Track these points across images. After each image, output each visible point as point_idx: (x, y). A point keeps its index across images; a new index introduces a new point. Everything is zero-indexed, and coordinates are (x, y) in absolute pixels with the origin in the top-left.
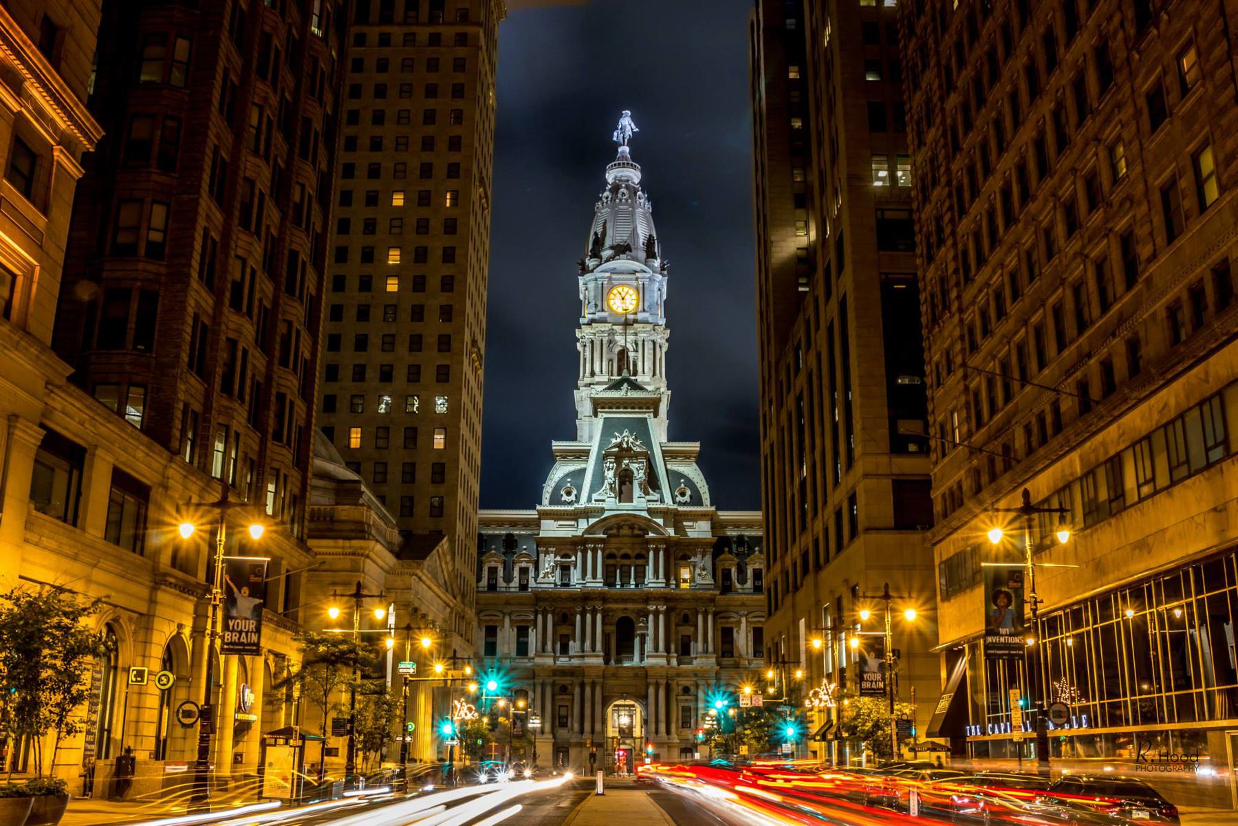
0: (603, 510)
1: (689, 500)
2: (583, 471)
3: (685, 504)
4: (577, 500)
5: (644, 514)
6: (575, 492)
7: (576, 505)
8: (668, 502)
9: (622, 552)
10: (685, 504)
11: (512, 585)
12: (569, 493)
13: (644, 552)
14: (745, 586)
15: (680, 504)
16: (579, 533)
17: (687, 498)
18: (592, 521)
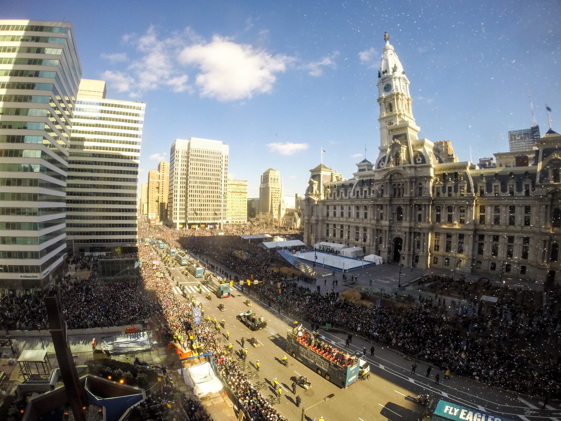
0: (388, 169)
3: (420, 163)
10: (420, 163)
15: (418, 164)
17: (420, 161)
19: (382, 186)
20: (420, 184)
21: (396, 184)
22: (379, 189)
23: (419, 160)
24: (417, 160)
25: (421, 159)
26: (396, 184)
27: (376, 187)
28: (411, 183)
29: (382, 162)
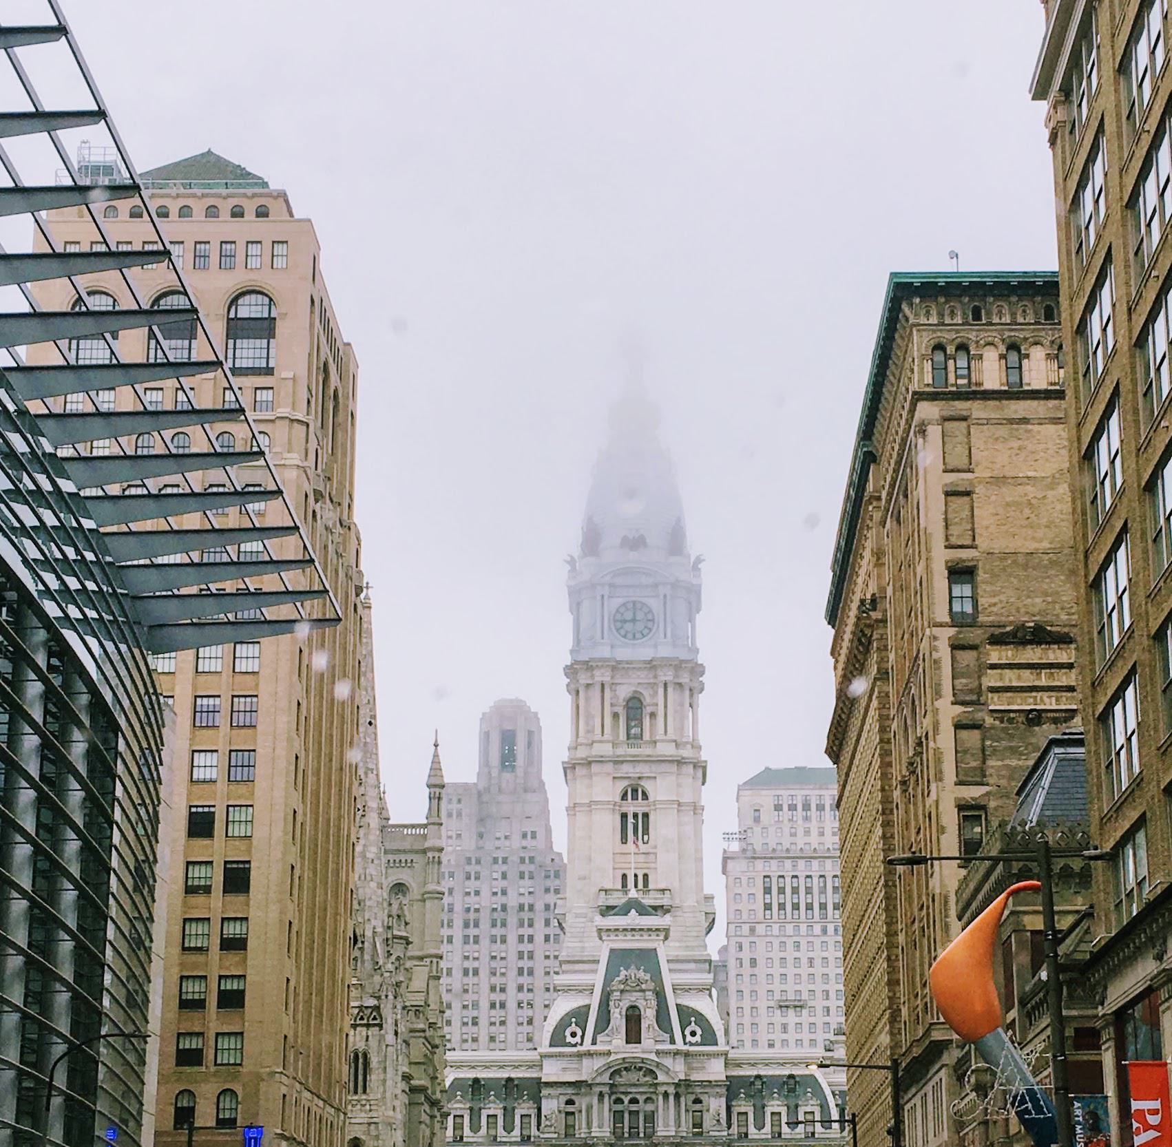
0: (609, 1053)
1: (699, 1040)
2: (588, 1007)
3: (696, 1044)
4: (581, 1044)
5: (653, 1057)
6: (579, 1033)
7: (579, 1048)
8: (680, 1045)
9: (629, 1098)
10: (696, 1044)
11: (513, 1134)
12: (573, 1035)
13: (654, 1097)
14: (763, 1131)
15: (691, 1044)
16: (583, 1078)
17: (698, 1038)
18: (599, 1063)
19: (570, 1102)
20: (697, 1101)
21: (626, 1100)
22: (560, 1112)
23: (693, 1034)
24: (687, 1032)
25: (699, 1032)
26: (626, 1100)
27: (551, 1105)
28: (677, 1096)
29: (573, 1028)
